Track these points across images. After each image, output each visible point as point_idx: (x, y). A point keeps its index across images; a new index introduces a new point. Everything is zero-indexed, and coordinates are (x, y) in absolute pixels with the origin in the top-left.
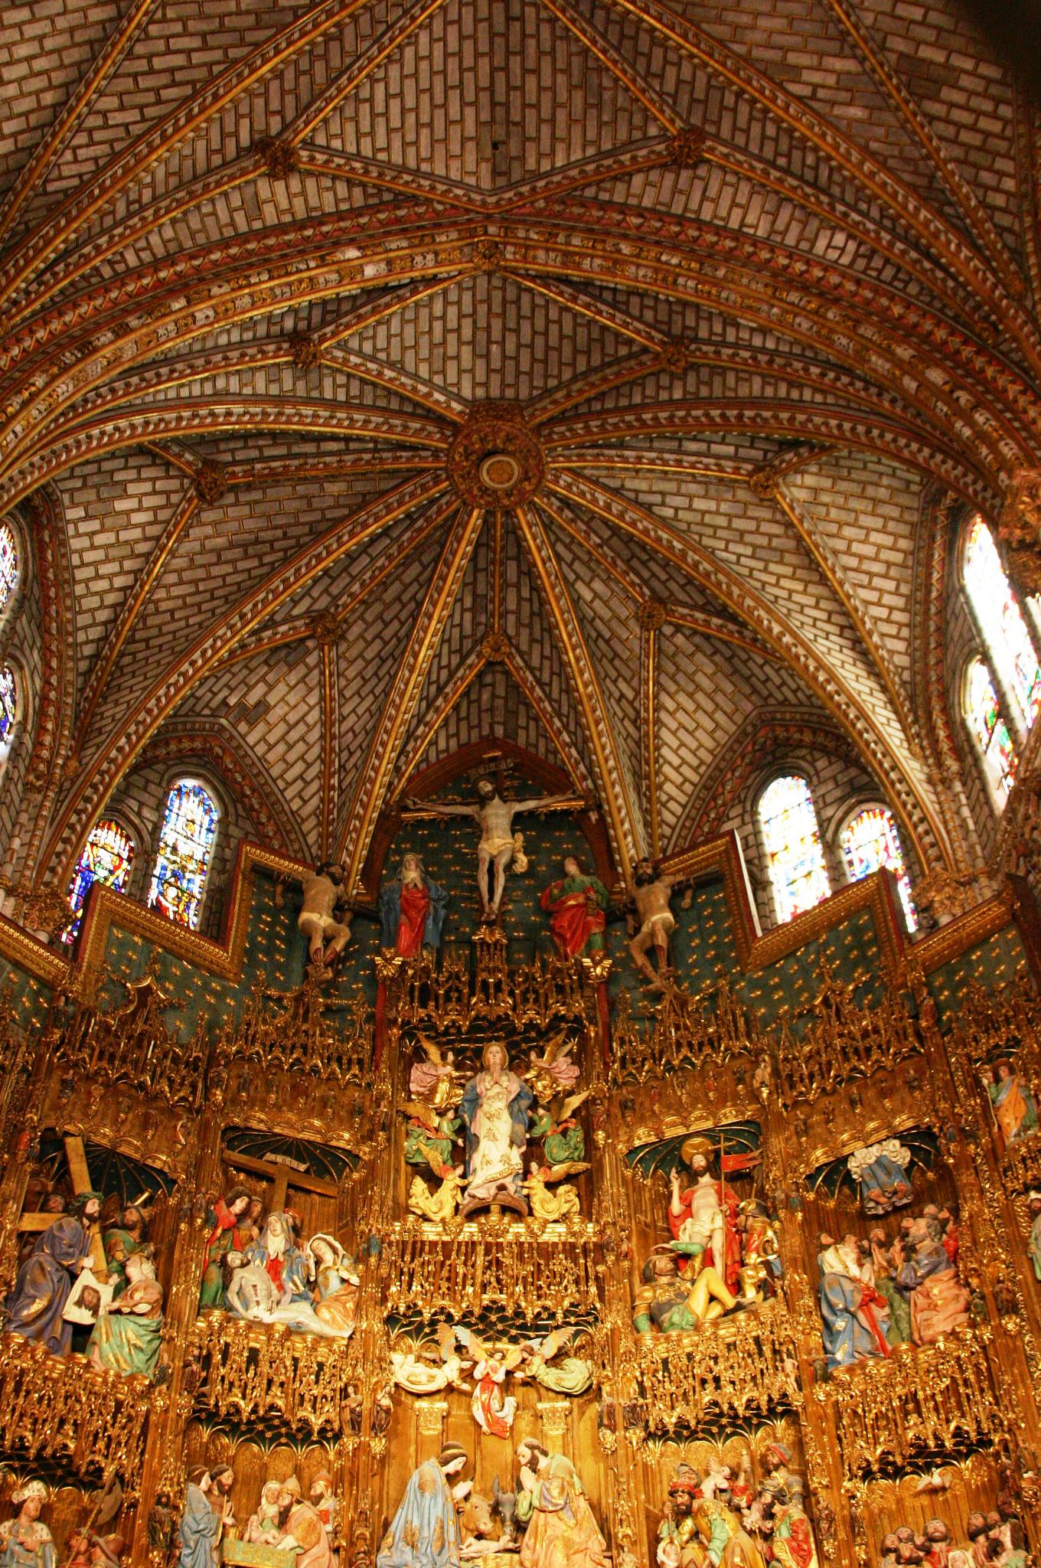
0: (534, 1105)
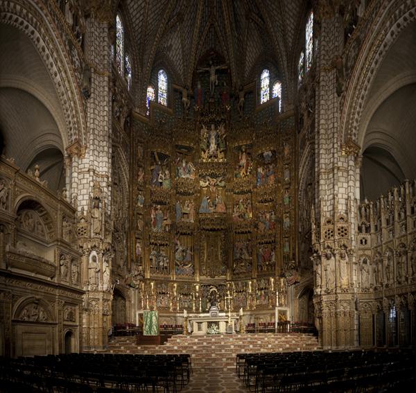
0: (218, 137)
